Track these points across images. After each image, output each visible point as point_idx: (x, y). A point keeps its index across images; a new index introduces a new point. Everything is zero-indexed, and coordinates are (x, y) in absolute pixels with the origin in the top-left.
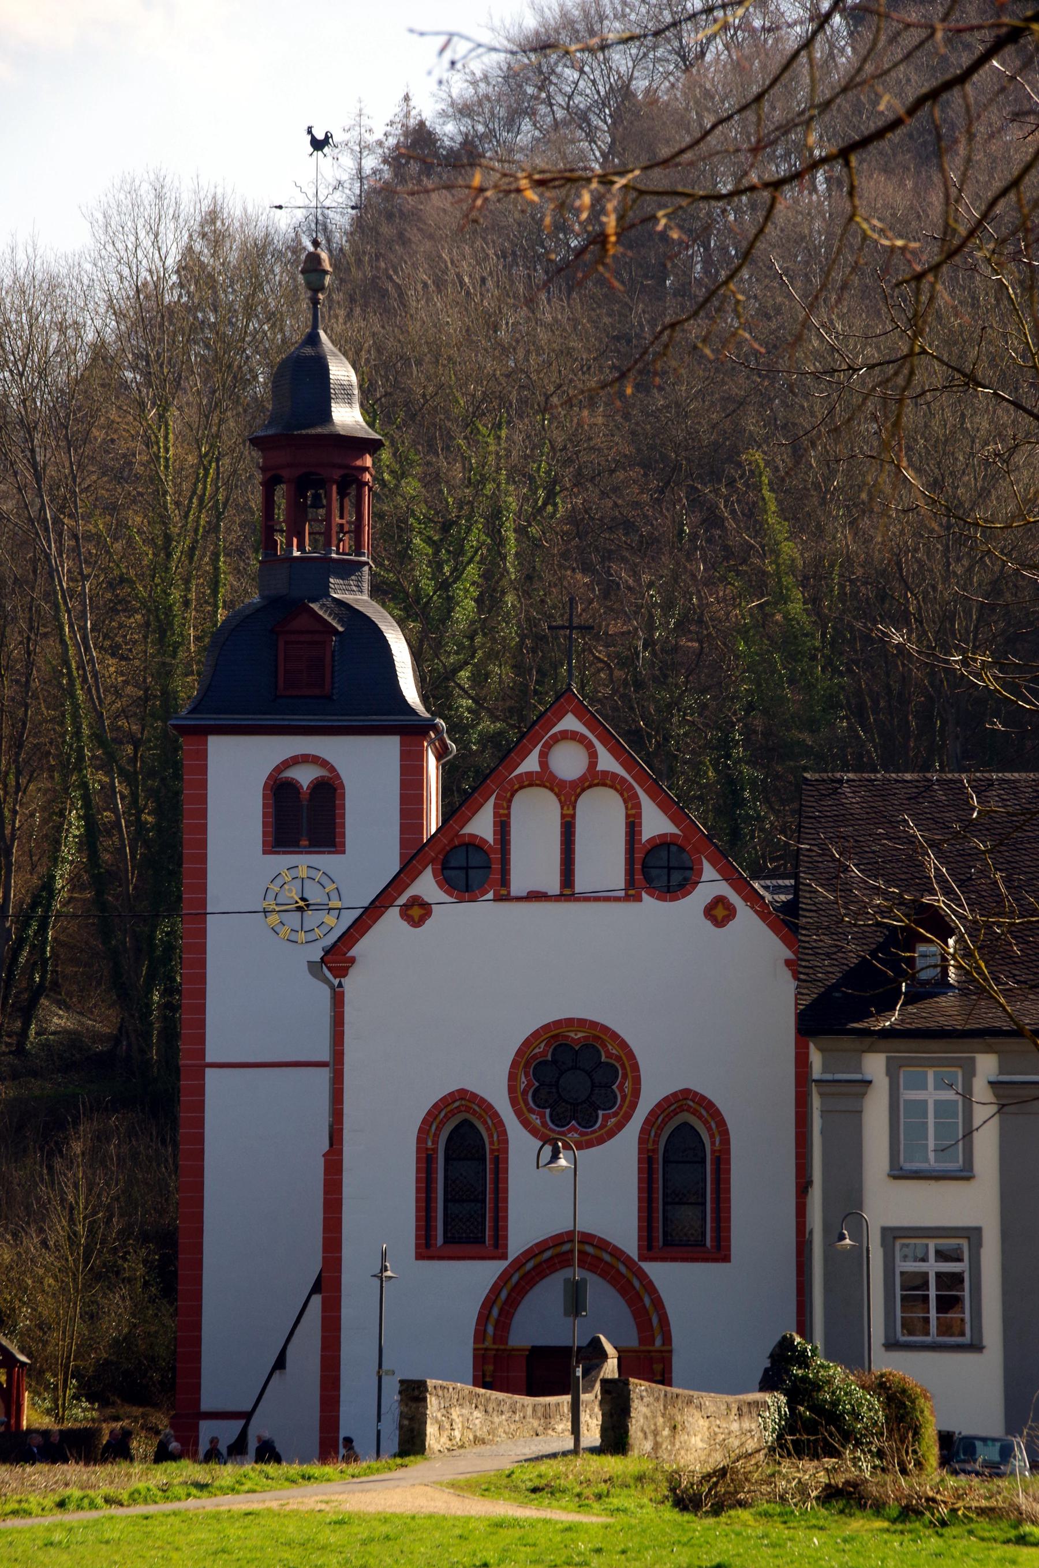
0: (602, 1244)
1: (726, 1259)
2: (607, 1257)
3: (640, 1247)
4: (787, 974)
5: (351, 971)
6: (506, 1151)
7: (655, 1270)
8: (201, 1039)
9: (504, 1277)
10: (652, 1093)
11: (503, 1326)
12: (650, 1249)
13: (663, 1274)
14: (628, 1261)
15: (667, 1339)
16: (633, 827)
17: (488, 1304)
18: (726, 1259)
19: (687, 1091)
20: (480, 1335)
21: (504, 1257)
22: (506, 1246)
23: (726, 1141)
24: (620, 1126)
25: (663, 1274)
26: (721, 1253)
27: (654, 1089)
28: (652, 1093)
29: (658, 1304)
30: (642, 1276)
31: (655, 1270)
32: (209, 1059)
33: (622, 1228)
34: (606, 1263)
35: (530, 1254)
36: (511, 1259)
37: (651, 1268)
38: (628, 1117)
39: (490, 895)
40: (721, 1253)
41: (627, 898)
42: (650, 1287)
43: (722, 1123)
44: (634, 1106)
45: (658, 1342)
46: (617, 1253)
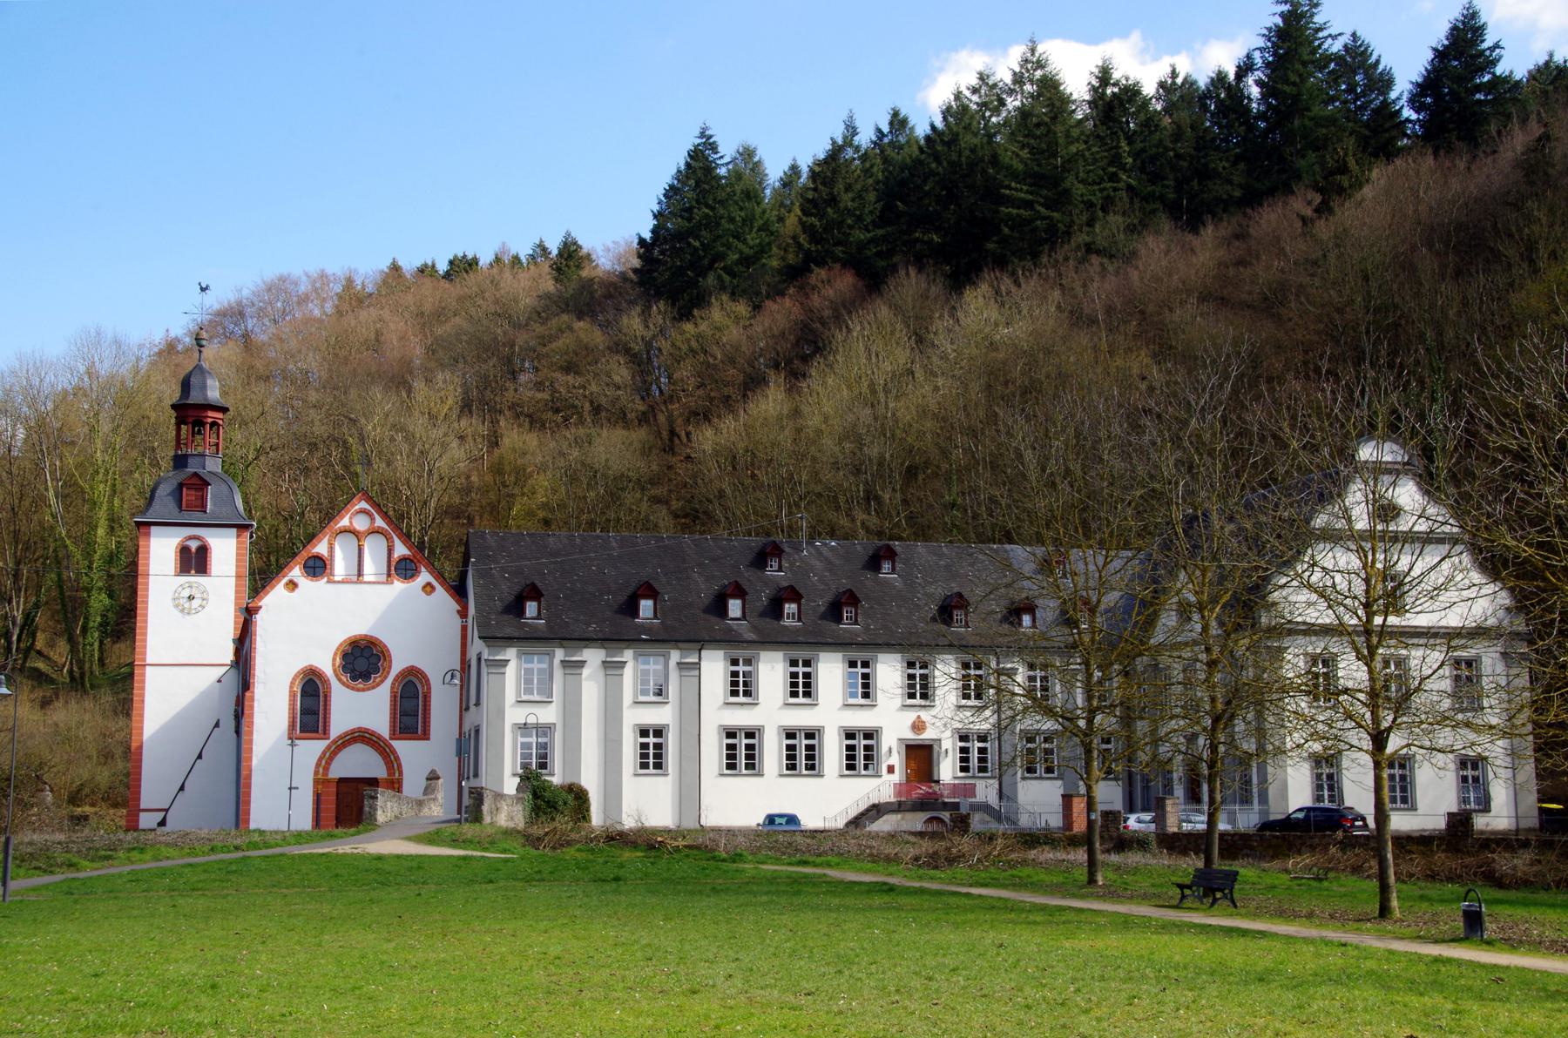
0: (373, 733)
7: (396, 744)
9: (329, 747)
11: (326, 769)
12: (394, 736)
13: (401, 746)
14: (384, 741)
15: (401, 773)
16: (390, 551)
17: (320, 759)
20: (316, 773)
23: (429, 688)
25: (401, 746)
26: (425, 736)
27: (398, 666)
28: (398, 666)
29: (397, 759)
30: (390, 746)
31: (396, 744)
32: (149, 661)
33: (380, 723)
35: (340, 737)
37: (395, 743)
40: (425, 736)
41: (387, 582)
42: (394, 752)
43: (427, 680)
46: (379, 737)
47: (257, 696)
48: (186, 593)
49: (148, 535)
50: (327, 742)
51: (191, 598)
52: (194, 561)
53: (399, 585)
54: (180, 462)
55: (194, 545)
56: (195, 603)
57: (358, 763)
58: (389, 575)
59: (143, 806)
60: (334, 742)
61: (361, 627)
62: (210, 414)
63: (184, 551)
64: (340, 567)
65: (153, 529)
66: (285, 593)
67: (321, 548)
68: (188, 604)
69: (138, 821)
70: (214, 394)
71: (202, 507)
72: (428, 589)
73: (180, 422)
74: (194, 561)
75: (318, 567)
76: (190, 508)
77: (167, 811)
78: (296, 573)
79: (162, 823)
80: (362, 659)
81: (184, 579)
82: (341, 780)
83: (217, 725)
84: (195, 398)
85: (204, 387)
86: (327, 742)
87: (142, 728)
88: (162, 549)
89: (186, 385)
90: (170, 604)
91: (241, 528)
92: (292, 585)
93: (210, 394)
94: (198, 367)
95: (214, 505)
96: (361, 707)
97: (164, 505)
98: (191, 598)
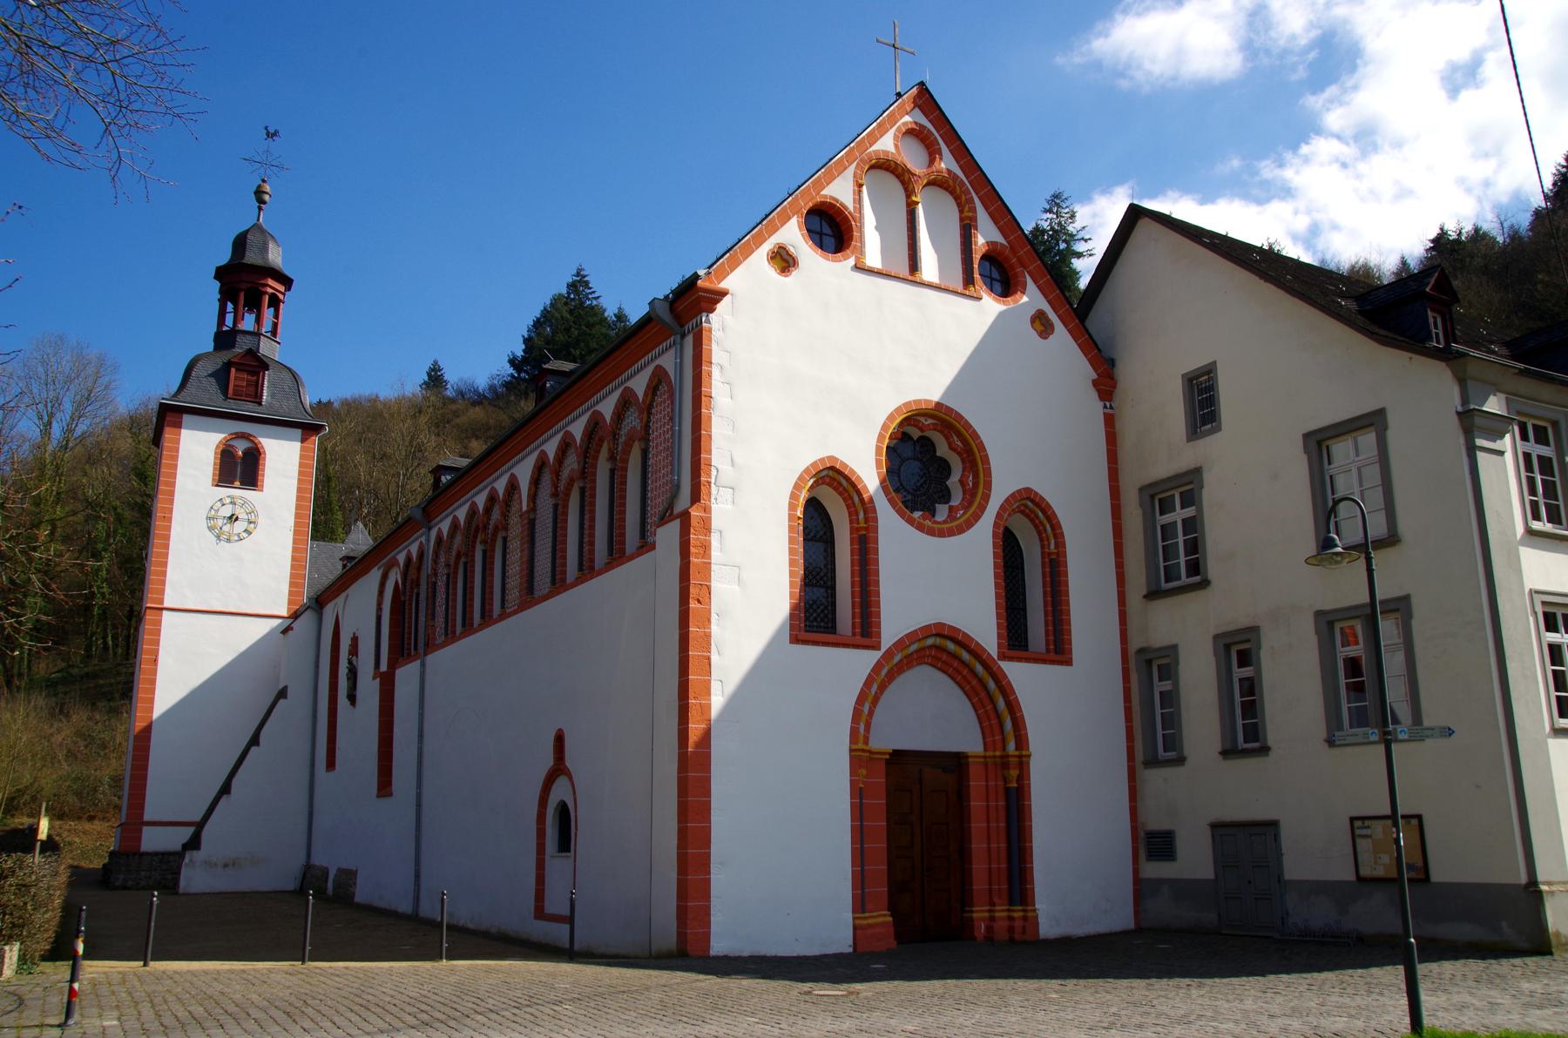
1: (1069, 663)
2: (965, 656)
3: (1000, 646)
4: (1094, 394)
5: (720, 307)
6: (876, 529)
8: (162, 592)
10: (1001, 490)
15: (1022, 741)
18: (1069, 663)
19: (1028, 490)
21: (876, 647)
22: (879, 635)
24: (977, 517)
28: (1001, 490)
29: (1013, 707)
32: (166, 605)
34: (963, 662)
35: (900, 644)
36: (884, 648)
38: (982, 509)
39: (852, 261)
42: (1006, 690)
44: (986, 498)
45: (1011, 746)
47: (715, 524)
48: (227, 511)
49: (179, 426)
50: (872, 657)
51: (233, 518)
52: (241, 468)
53: (990, 307)
54: (224, 339)
55: (240, 447)
56: (239, 527)
57: (933, 718)
58: (968, 280)
59: (146, 818)
60: (889, 654)
61: (931, 387)
62: (270, 282)
64: (872, 243)
65: (186, 418)
66: (771, 272)
67: (840, 190)
68: (226, 527)
69: (139, 839)
71: (257, 398)
72: (1041, 324)
73: (227, 295)
74: (241, 468)
75: (833, 230)
76: (238, 396)
77: (200, 826)
78: (792, 234)
79: (194, 843)
80: (931, 457)
81: (224, 492)
82: (898, 755)
83: (282, 694)
84: (251, 258)
85: (265, 249)
86: (872, 657)
87: (152, 700)
88: (196, 449)
89: (240, 243)
91: (308, 430)
92: (784, 261)
93: (271, 256)
94: (257, 227)
95: (273, 395)
96: (936, 579)
97: (206, 393)
98: (233, 518)
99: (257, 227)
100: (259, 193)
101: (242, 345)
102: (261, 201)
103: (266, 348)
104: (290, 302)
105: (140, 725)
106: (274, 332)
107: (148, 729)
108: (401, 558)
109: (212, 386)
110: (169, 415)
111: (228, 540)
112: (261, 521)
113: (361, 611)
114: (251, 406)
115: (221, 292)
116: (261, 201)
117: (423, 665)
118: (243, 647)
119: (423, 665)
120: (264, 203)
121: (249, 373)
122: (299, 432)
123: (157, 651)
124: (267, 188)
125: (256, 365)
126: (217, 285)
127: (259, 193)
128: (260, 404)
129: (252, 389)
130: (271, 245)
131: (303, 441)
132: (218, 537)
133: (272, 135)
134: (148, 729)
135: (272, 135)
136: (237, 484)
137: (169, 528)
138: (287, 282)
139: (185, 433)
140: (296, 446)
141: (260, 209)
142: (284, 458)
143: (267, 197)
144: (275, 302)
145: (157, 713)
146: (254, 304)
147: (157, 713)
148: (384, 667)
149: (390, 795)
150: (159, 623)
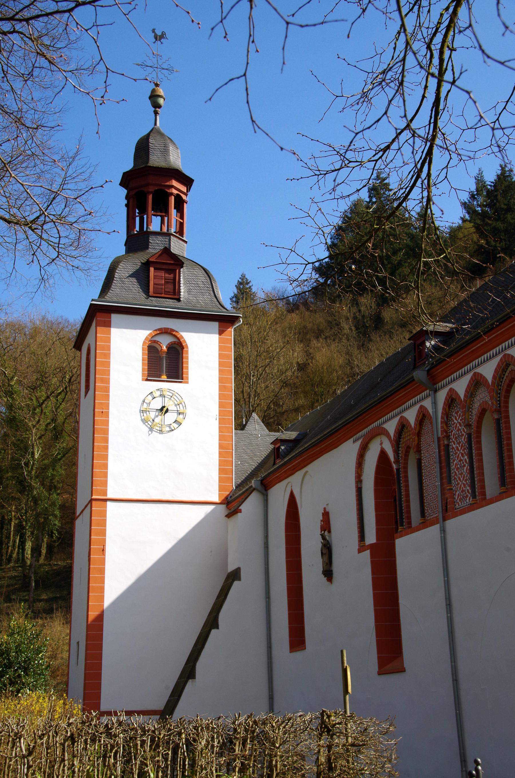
32: (110, 496)
48: (157, 404)
49: (108, 325)
51: (164, 410)
52: (166, 362)
54: (136, 242)
55: (165, 342)
56: (170, 418)
62: (175, 183)
63: (152, 350)
65: (115, 317)
68: (160, 418)
70: (176, 159)
71: (176, 295)
74: (166, 362)
76: (158, 295)
81: (154, 386)
84: (155, 160)
85: (165, 152)
87: (102, 590)
88: (126, 345)
89: (143, 148)
90: (137, 417)
91: (224, 321)
95: (189, 292)
97: (127, 291)
98: (164, 410)
99: (154, 131)
100: (154, 97)
101: (156, 245)
102: (156, 106)
103: (177, 247)
104: (193, 200)
105: (93, 614)
106: (181, 231)
107: (100, 617)
108: (391, 426)
109: (134, 285)
110: (99, 314)
111: (161, 432)
112: (189, 411)
113: (333, 485)
114: (171, 302)
115: (127, 198)
116: (156, 106)
117: (443, 530)
118: (181, 534)
119: (443, 530)
120: (160, 107)
121: (168, 271)
122: (215, 325)
123: (104, 540)
124: (161, 91)
125: (172, 263)
126: (124, 192)
127: (154, 97)
128: (179, 300)
129: (170, 287)
130: (171, 148)
131: (221, 333)
132: (151, 429)
133: (159, 38)
134: (100, 617)
135: (159, 38)
136: (164, 377)
137: (107, 423)
138: (188, 182)
139: (114, 331)
140: (215, 338)
141: (156, 113)
142: (205, 349)
143: (161, 101)
144: (180, 204)
145: (107, 603)
146: (161, 208)
147: (107, 603)
148: (371, 538)
149: (403, 670)
150: (104, 514)
